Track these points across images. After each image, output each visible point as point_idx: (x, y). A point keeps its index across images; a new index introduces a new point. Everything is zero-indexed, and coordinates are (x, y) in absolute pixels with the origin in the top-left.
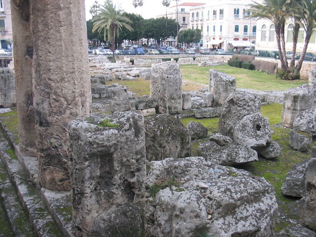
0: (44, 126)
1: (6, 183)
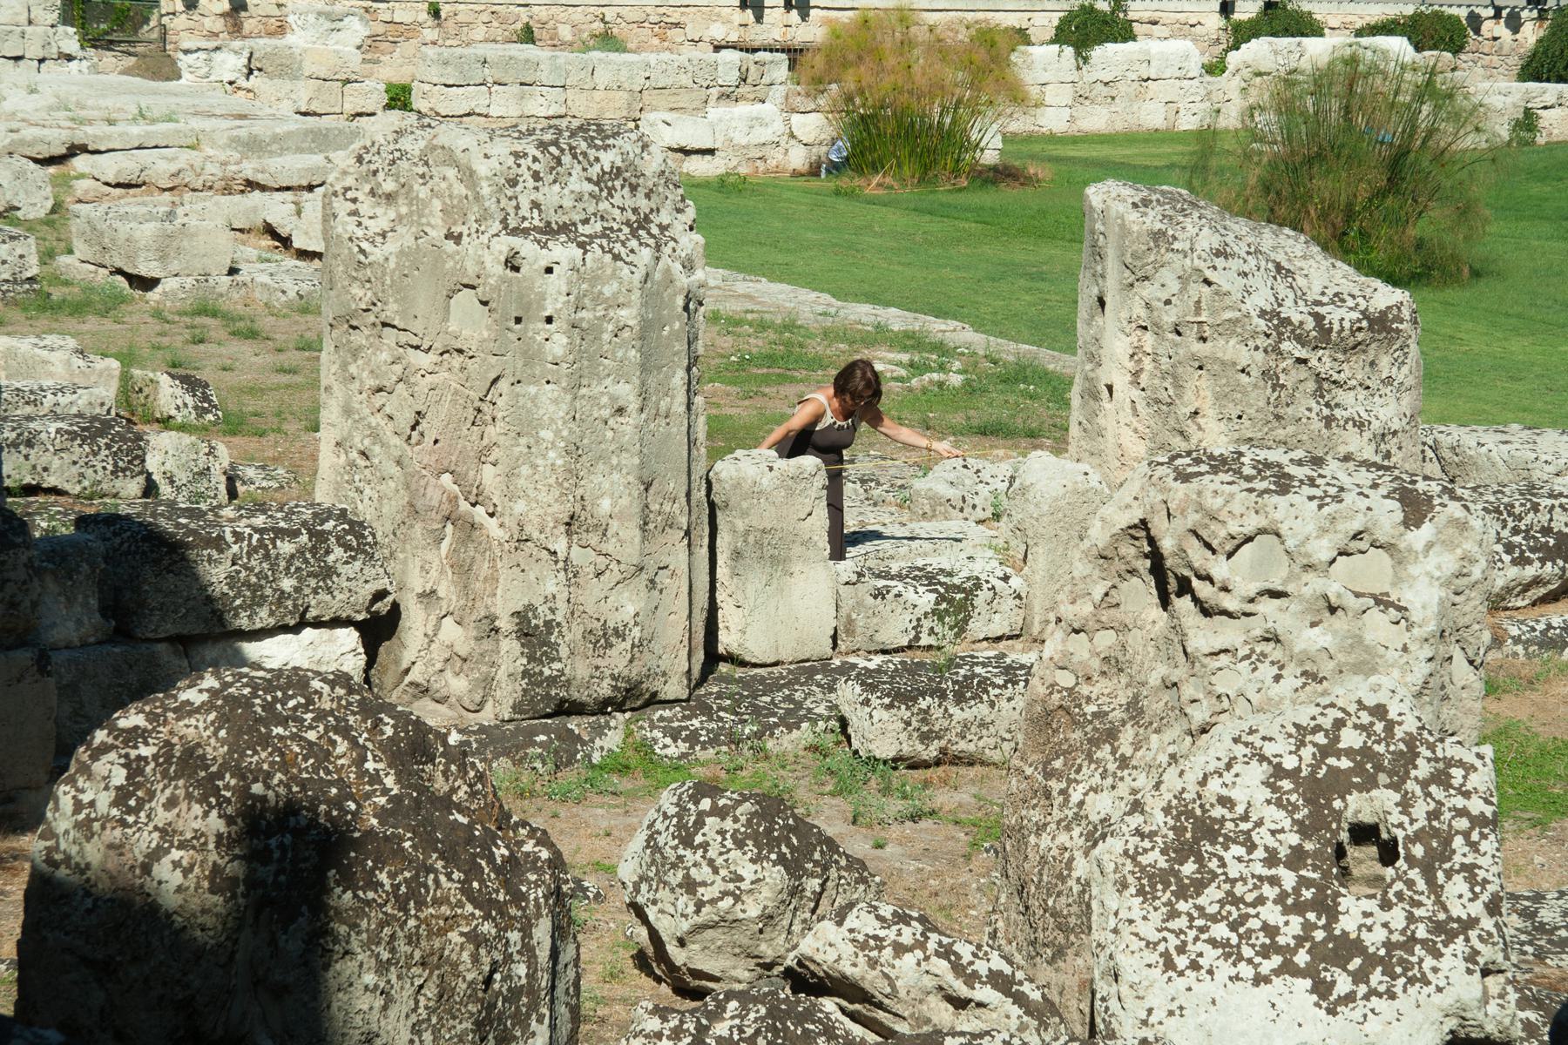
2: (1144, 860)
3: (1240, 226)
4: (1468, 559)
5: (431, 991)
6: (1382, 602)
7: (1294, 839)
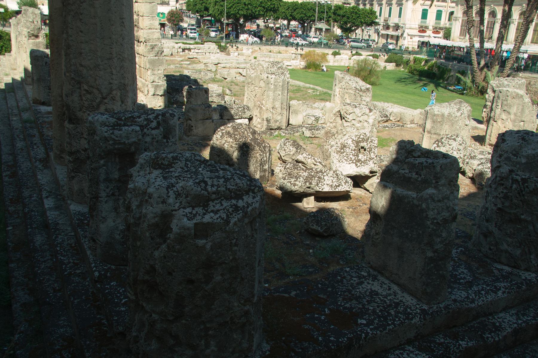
0: (74, 124)
1: (33, 197)
3: (352, 77)
4: (376, 117)
5: (255, 160)
6: (366, 121)
7: (354, 148)
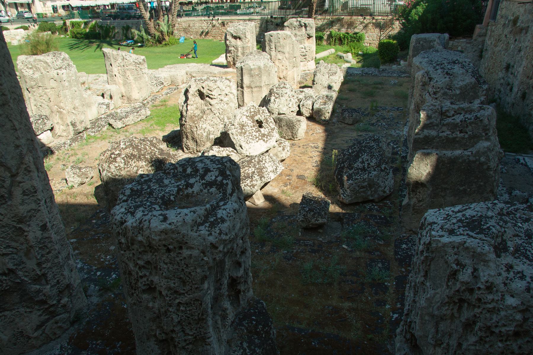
2: (238, 131)
7: (252, 124)
